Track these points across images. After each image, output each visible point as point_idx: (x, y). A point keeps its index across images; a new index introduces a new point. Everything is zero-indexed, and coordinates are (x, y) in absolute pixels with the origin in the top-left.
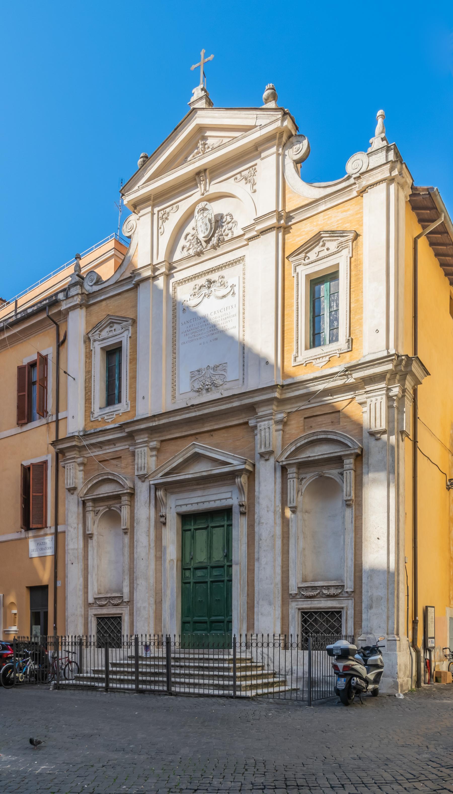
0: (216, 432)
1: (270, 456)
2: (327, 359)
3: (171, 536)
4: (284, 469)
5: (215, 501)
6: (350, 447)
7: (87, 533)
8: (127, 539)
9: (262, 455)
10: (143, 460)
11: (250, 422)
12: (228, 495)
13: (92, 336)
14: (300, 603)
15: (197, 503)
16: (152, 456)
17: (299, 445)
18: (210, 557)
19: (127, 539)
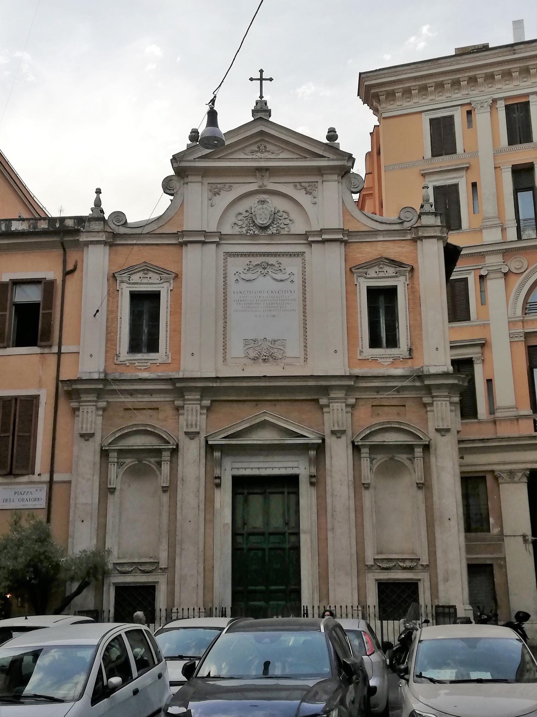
0: (279, 403)
1: (341, 434)
3: (224, 498)
4: (356, 449)
5: (279, 468)
7: (109, 486)
9: (333, 433)
10: (194, 418)
12: (295, 464)
13: (120, 277)
14: (376, 574)
15: (259, 468)
18: (267, 523)
19: (165, 498)
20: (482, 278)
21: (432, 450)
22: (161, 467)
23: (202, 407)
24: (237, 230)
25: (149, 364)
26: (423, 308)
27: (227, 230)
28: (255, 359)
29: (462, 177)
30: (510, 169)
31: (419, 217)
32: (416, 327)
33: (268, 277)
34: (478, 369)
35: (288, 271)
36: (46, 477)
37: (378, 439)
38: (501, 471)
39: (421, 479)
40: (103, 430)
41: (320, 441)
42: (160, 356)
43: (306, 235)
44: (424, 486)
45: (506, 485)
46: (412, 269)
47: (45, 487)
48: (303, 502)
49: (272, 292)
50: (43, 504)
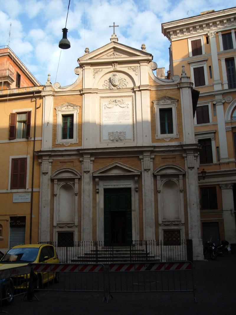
2: (170, 139)
4: (155, 176)
5: (123, 185)
6: (182, 171)
7: (54, 193)
8: (77, 198)
9: (145, 170)
11: (140, 157)
16: (91, 164)
17: (162, 168)
20: (214, 105)
21: (187, 176)
22: (75, 185)
23: (91, 161)
24: (104, 88)
25: (69, 144)
26: (183, 117)
27: (101, 87)
28: (113, 140)
29: (205, 64)
30: (224, 60)
31: (181, 79)
32: (180, 124)
33: (118, 106)
34: (213, 143)
35: (127, 103)
36: (30, 190)
37: (164, 172)
38: (222, 184)
39: (182, 188)
40: (52, 171)
41: (140, 174)
42: (75, 140)
43: (133, 89)
44: (184, 191)
45: (224, 190)
46: (178, 100)
47: (30, 194)
48: (133, 199)
49: (120, 112)
50: (29, 200)
